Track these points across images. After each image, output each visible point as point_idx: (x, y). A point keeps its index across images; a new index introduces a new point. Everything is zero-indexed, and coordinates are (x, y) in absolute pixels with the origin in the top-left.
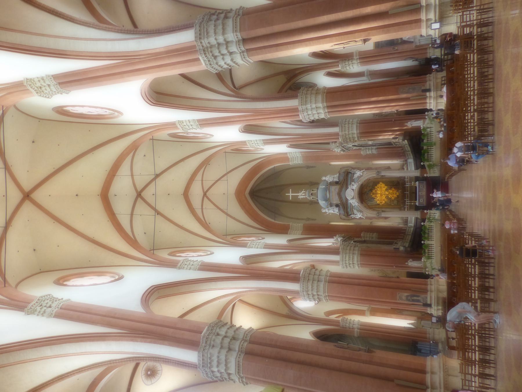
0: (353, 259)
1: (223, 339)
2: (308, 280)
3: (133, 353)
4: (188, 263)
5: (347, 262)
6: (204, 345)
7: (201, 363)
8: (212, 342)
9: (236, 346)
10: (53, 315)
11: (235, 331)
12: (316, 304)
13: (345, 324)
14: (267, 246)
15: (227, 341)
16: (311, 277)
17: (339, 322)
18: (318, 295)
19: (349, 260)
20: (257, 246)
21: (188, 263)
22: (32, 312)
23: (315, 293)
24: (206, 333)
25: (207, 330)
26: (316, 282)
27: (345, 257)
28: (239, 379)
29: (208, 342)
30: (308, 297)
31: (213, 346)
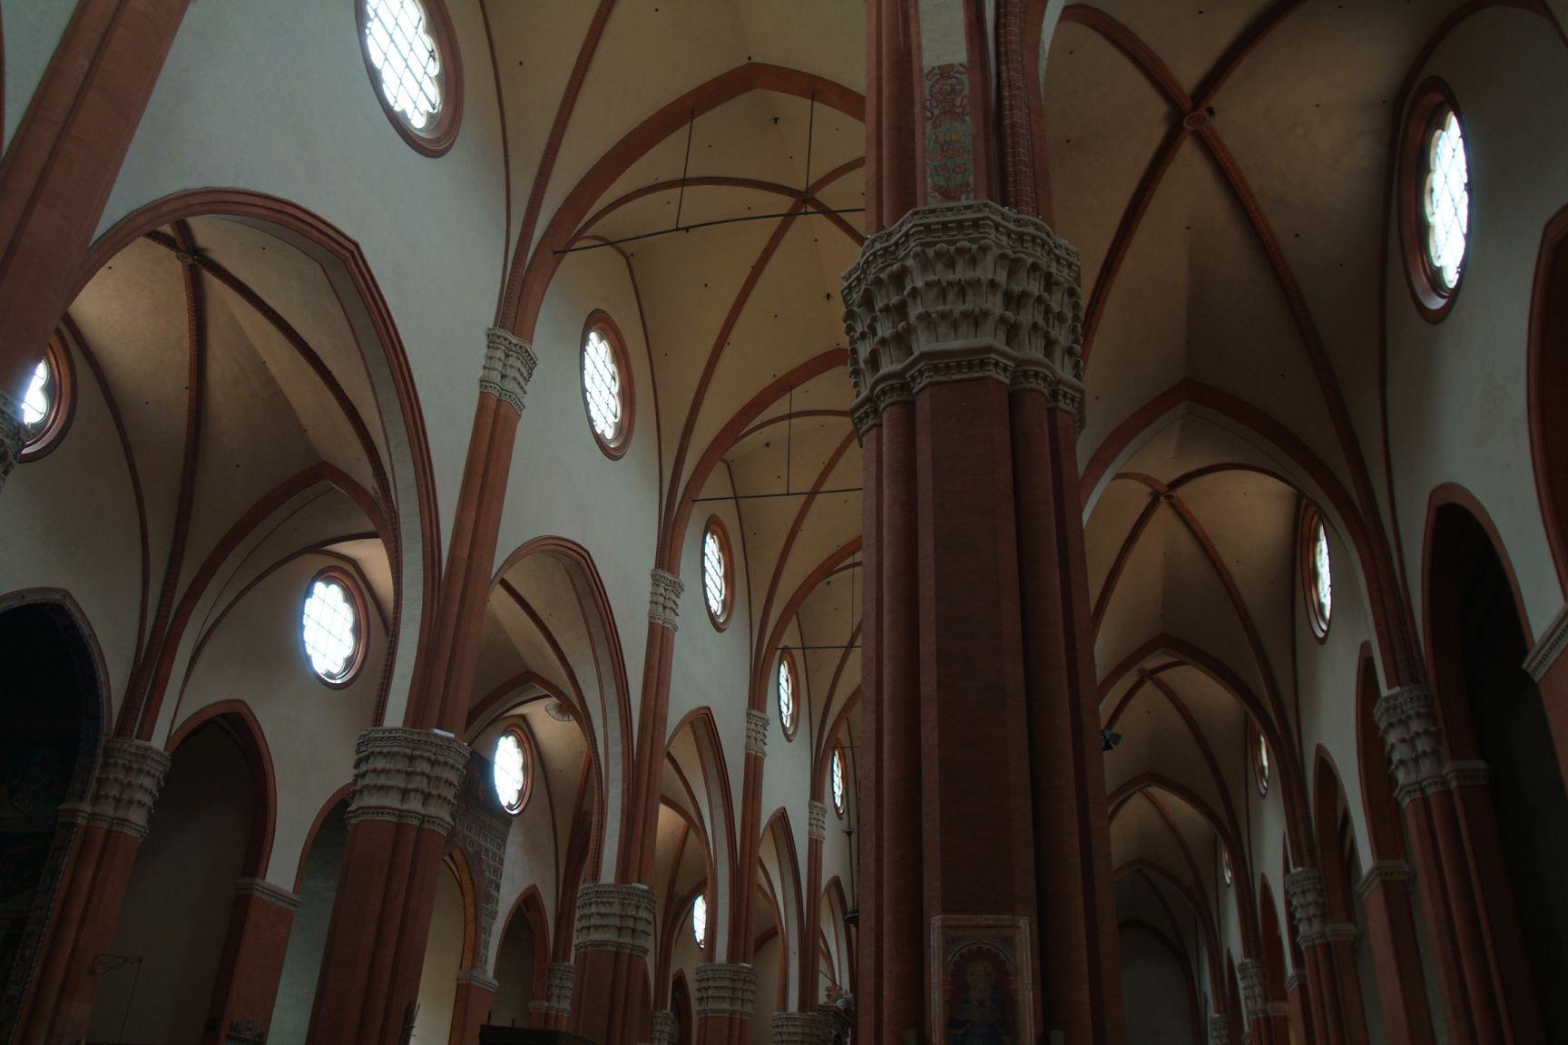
0: (791, 1041)
1: (632, 916)
2: (734, 980)
3: (607, 776)
4: (760, 729)
5: (785, 1029)
6: (624, 890)
7: (601, 889)
8: (627, 902)
9: (626, 939)
10: (653, 621)
11: (642, 931)
12: (698, 944)
13: (659, 1021)
14: (815, 846)
15: (630, 923)
16: (739, 985)
17: (662, 1009)
18: (708, 998)
19: (789, 1033)
20: (815, 822)
21: (760, 729)
22: (656, 583)
23: (710, 993)
24: (638, 889)
25: (643, 891)
26: (728, 994)
27: (796, 1026)
28: (584, 943)
29: (627, 897)
30: (704, 979)
31: (623, 904)
